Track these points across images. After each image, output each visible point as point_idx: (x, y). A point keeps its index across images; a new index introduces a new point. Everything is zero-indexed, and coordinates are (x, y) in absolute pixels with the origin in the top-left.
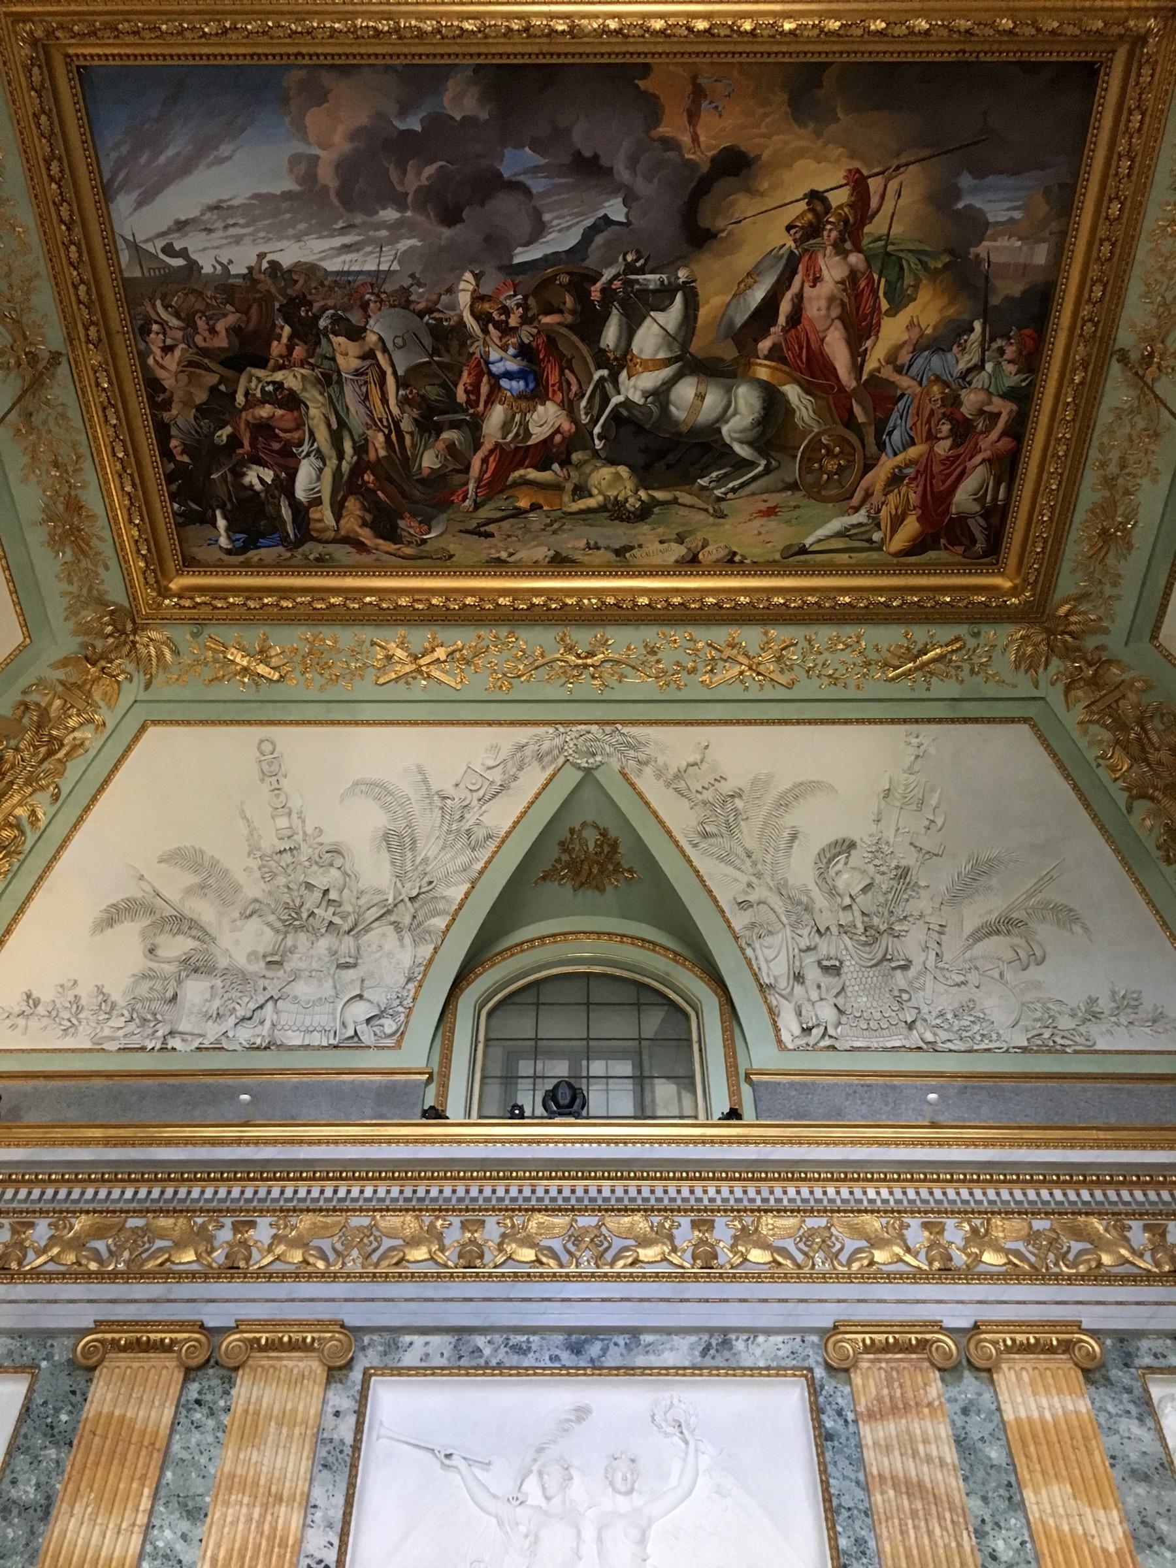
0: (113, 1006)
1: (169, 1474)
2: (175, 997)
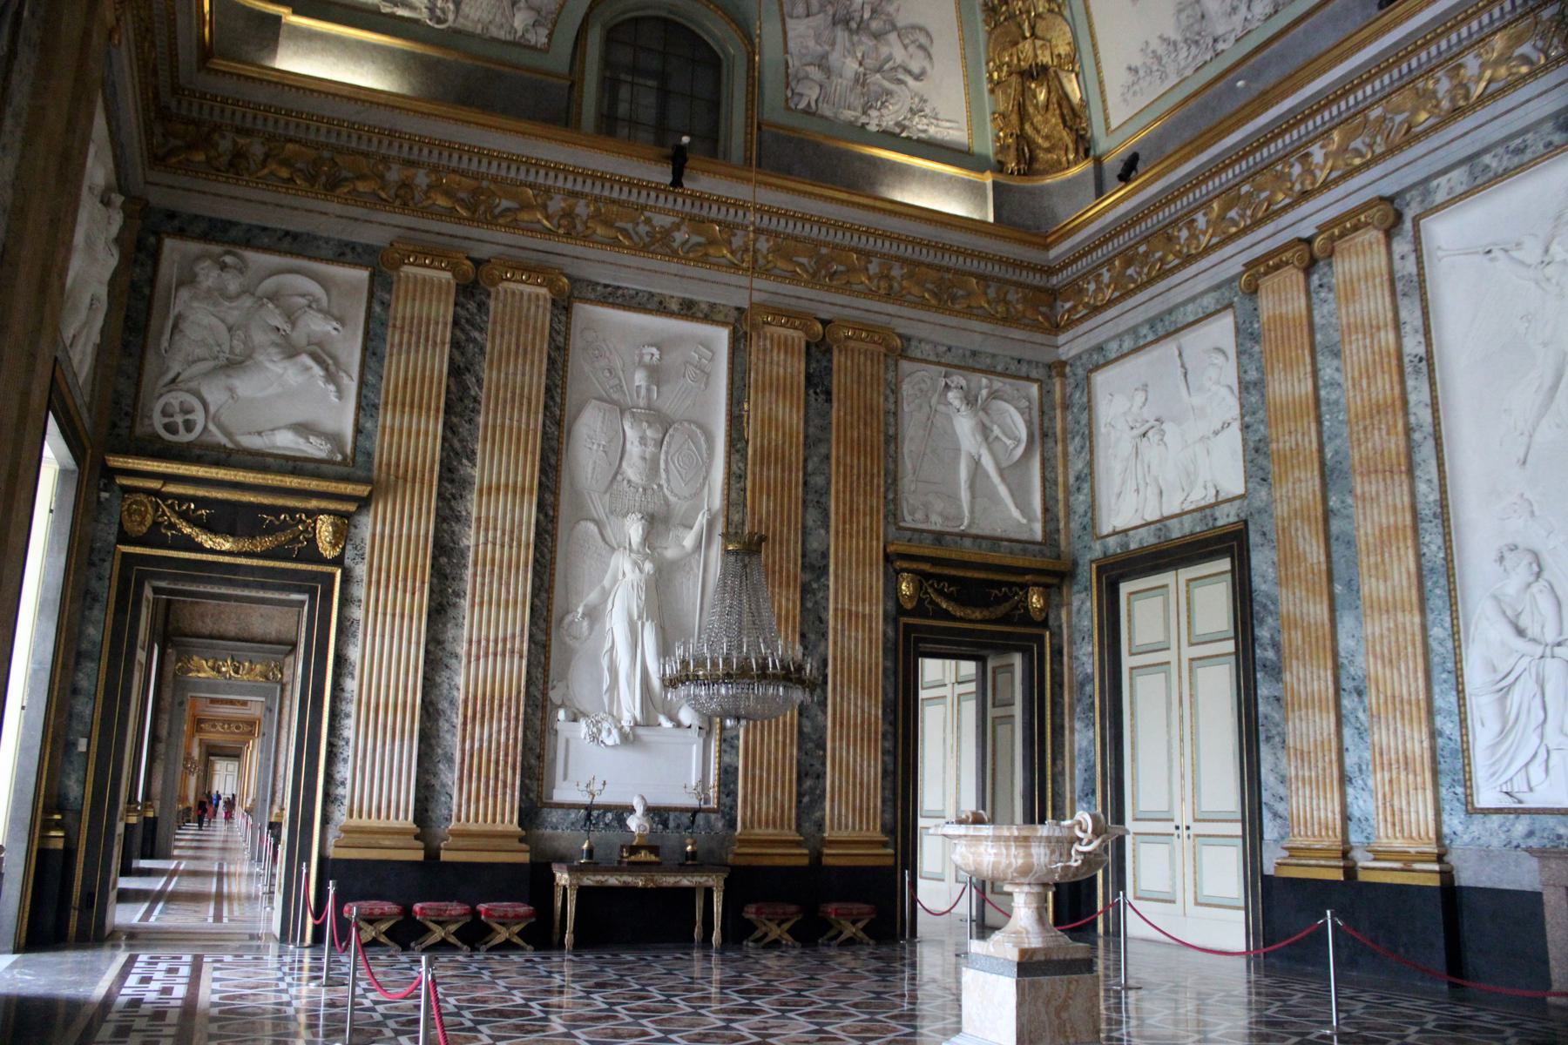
0: (1175, 43)
1: (1319, 337)
2: (1203, 17)
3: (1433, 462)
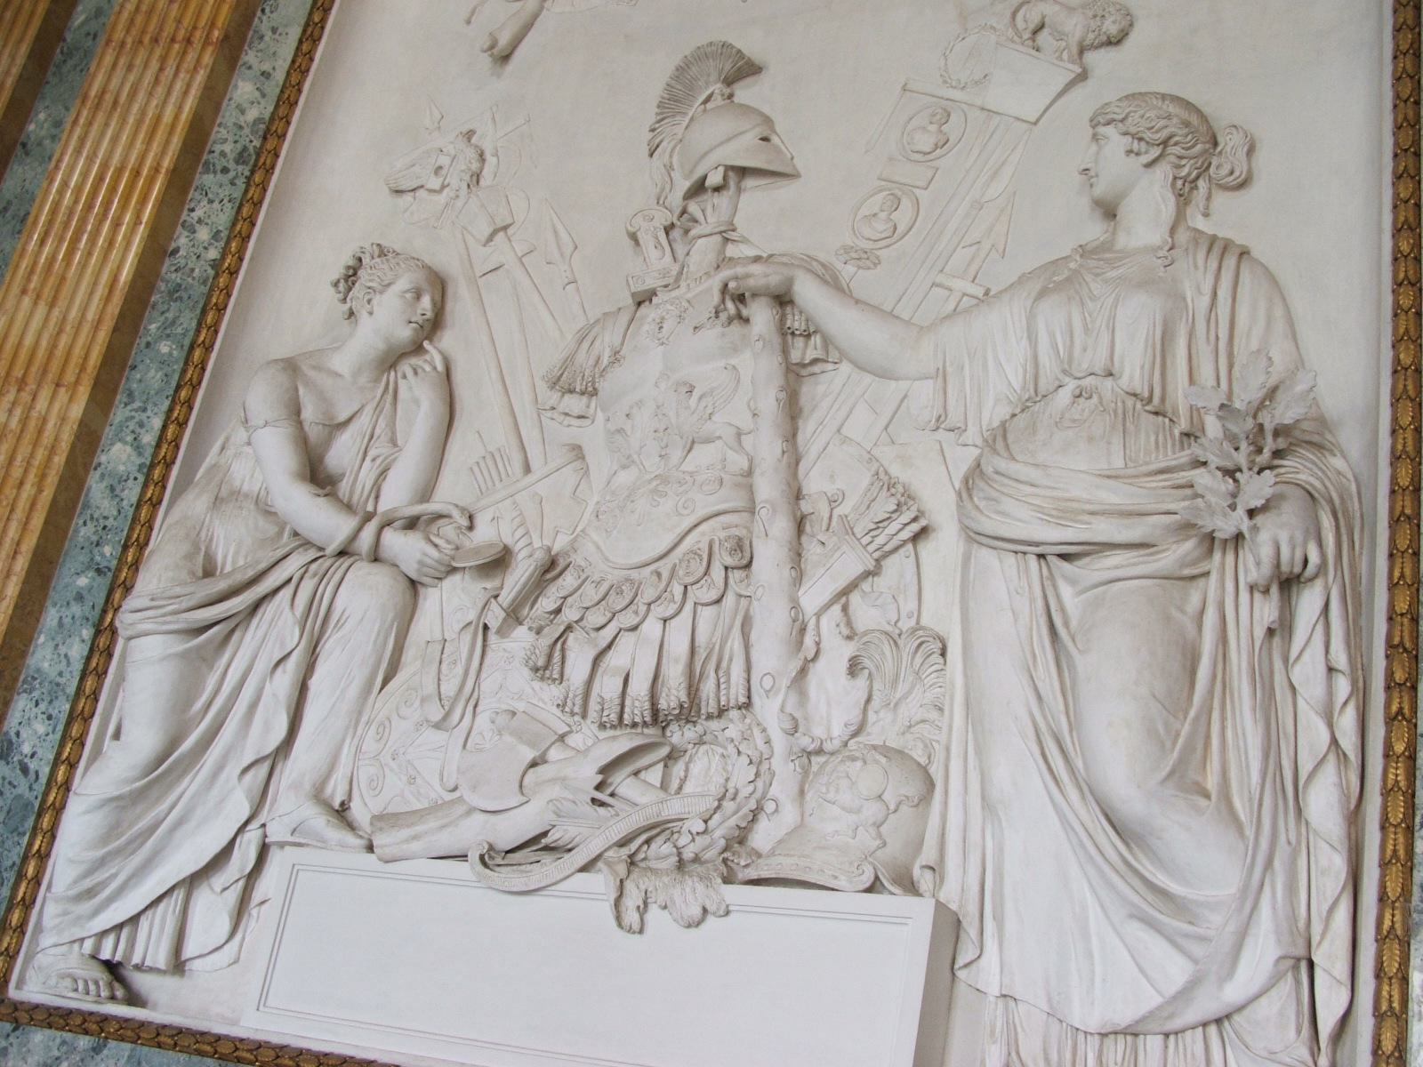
3: (295, 32)
